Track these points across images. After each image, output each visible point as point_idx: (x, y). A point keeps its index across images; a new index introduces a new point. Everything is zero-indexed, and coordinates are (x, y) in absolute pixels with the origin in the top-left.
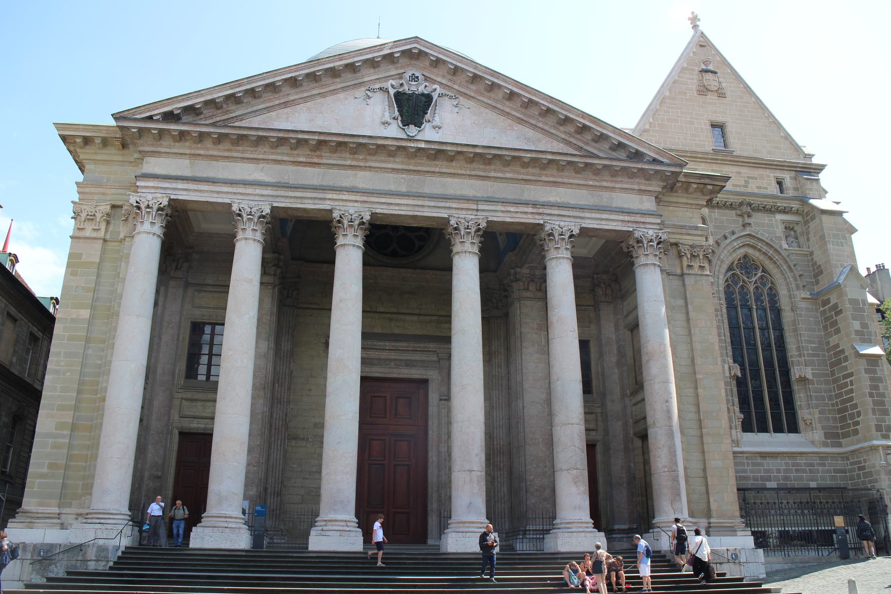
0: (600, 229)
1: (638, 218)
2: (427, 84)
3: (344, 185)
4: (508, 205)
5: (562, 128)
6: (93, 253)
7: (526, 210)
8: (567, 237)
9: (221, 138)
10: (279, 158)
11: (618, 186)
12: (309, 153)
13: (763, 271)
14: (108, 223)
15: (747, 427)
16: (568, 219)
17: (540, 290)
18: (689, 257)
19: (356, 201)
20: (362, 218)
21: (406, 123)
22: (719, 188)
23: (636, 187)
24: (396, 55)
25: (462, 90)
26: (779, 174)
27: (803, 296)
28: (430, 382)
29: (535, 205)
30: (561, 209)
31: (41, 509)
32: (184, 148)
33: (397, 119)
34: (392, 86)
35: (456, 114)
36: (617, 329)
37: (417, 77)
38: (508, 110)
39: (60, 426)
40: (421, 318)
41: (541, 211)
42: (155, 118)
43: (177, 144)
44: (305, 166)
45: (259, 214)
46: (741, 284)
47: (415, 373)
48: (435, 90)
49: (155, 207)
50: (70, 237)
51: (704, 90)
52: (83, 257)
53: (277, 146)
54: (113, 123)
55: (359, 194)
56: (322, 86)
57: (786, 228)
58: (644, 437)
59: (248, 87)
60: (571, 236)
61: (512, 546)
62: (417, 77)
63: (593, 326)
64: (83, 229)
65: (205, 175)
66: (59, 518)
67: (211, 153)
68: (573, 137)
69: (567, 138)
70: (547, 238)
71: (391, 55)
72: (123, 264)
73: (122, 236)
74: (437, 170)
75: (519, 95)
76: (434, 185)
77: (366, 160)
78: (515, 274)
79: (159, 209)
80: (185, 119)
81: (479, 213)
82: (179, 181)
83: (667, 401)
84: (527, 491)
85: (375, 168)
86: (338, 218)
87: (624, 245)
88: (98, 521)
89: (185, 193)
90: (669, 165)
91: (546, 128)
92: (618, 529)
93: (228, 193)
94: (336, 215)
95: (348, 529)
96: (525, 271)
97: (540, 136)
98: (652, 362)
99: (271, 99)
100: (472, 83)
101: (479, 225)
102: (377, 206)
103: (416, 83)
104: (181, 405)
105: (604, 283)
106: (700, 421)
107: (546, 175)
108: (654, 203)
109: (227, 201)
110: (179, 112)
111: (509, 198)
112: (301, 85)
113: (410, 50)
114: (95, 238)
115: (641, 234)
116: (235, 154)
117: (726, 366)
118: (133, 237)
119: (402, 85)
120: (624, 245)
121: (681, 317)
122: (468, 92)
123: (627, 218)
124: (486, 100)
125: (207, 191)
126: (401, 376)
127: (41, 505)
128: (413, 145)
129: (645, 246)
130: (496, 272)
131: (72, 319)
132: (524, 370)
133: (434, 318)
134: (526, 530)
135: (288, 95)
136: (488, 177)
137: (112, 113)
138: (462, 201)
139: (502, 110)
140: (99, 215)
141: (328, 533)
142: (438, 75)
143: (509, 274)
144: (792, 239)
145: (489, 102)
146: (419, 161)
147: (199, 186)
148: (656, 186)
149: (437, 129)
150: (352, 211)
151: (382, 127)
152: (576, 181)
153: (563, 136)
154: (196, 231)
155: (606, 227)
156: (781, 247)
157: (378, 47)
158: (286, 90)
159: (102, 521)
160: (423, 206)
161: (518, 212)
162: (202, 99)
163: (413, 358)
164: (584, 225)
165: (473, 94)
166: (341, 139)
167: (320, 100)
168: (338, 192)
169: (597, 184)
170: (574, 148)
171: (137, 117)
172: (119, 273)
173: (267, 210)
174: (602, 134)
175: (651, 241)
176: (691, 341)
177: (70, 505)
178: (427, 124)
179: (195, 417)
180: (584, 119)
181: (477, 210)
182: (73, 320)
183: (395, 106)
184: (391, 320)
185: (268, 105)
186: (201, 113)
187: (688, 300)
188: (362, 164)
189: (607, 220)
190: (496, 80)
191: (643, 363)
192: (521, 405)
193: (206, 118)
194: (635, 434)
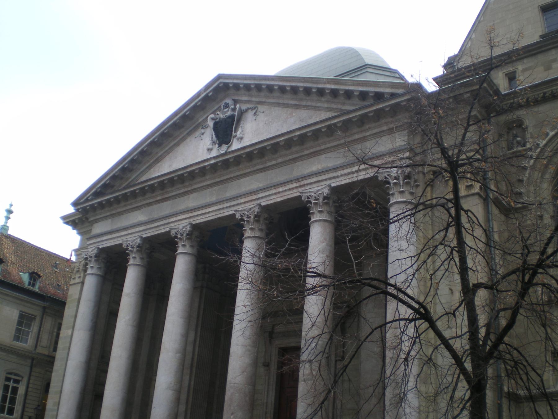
5: (323, 99)
10: (148, 201)
11: (368, 134)
19: (185, 219)
21: (220, 145)
23: (385, 128)
25: (257, 100)
29: (297, 180)
34: (212, 119)
41: (302, 183)
42: (89, 199)
44: (162, 202)
49: (93, 256)
54: (72, 210)
71: (208, 94)
74: (232, 175)
76: (233, 189)
77: (191, 185)
91: (314, 104)
94: (173, 234)
107: (307, 149)
113: (218, 85)
115: (386, 174)
116: (128, 207)
135: (157, 153)
149: (240, 140)
160: (223, 209)
161: (285, 191)
162: (108, 177)
168: (176, 216)
180: (330, 84)
181: (257, 199)
185: (147, 165)
188: (189, 189)
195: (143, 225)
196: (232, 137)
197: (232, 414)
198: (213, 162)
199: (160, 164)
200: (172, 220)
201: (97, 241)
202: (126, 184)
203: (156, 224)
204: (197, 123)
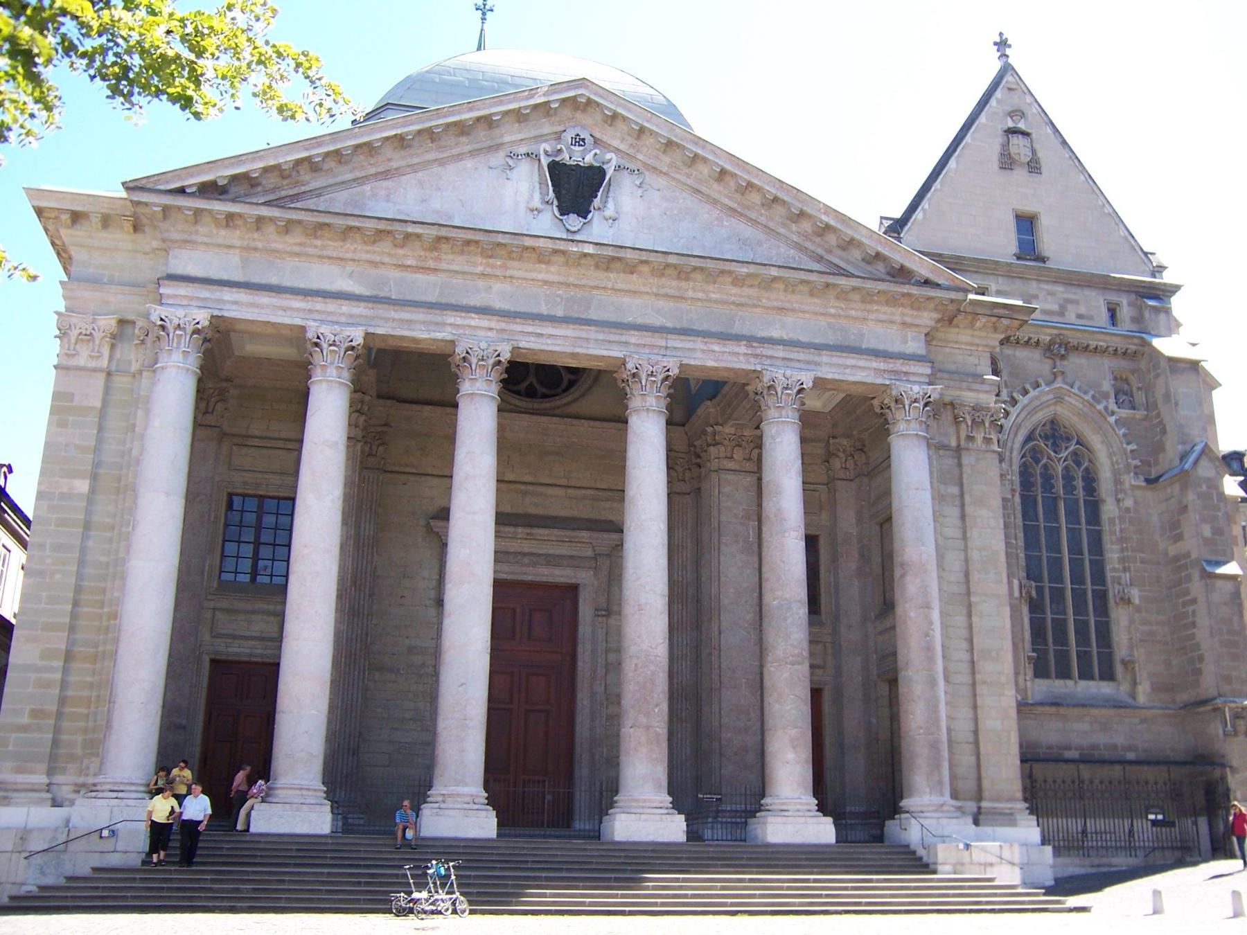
0: (842, 381)
1: (898, 365)
2: (598, 152)
3: (472, 304)
4: (713, 340)
5: (794, 227)
6: (91, 393)
7: (736, 349)
8: (795, 391)
9: (288, 227)
10: (377, 258)
12: (422, 253)
13: (1078, 443)
14: (113, 347)
15: (1041, 671)
16: (797, 365)
17: (750, 459)
18: (970, 424)
19: (491, 329)
20: (499, 355)
21: (564, 211)
22: (1019, 322)
23: (898, 318)
24: (554, 106)
26: (1114, 297)
27: (1133, 483)
28: (581, 589)
30: (787, 348)
31: (21, 778)
34: (546, 152)
35: (639, 199)
36: (859, 521)
37: (583, 140)
38: (716, 196)
39: (48, 654)
40: (570, 491)
41: (758, 351)
44: (415, 272)
45: (347, 344)
46: (1045, 461)
47: (560, 575)
48: (610, 161)
49: (190, 329)
50: (55, 367)
51: (1007, 162)
52: (77, 398)
53: (374, 242)
54: (124, 194)
56: (441, 148)
57: (1115, 379)
58: (893, 682)
59: (332, 148)
60: (800, 391)
61: (697, 832)
62: (583, 140)
63: (824, 515)
65: (264, 281)
66: (48, 791)
67: (274, 245)
68: (811, 240)
69: (800, 241)
70: (765, 392)
71: (549, 102)
72: (140, 413)
73: (134, 367)
75: (734, 175)
78: (714, 434)
80: (234, 190)
81: (668, 353)
82: (226, 288)
83: (927, 635)
84: (721, 754)
87: (876, 402)
88: (115, 795)
89: (234, 307)
90: (948, 289)
91: (771, 225)
92: (851, 813)
93: (299, 310)
94: (460, 350)
95: (476, 807)
96: (728, 429)
97: (762, 236)
98: (908, 578)
100: (664, 152)
101: (668, 370)
102: (521, 338)
103: (581, 148)
104: (213, 619)
105: (844, 451)
106: (973, 662)
107: (768, 299)
108: (923, 345)
109: (298, 322)
110: (225, 182)
112: (410, 146)
113: (575, 97)
114: (95, 370)
115: (902, 389)
116: (310, 251)
117: (1016, 582)
118: (154, 371)
119: (560, 151)
120: (876, 402)
121: (953, 512)
122: (657, 164)
123: (882, 365)
124: (683, 178)
125: (268, 306)
126: (538, 579)
127: (20, 770)
128: (575, 249)
129: (907, 407)
130: (683, 425)
131: (62, 493)
132: (723, 579)
133: (589, 492)
134: (718, 812)
135: (390, 160)
137: (124, 180)
139: (708, 196)
140: (98, 335)
141: (447, 812)
142: (613, 137)
143: (704, 433)
144: (1124, 397)
145: (689, 182)
146: (583, 272)
147: (256, 298)
148: (927, 318)
150: (483, 345)
151: (530, 215)
152: (812, 308)
153: (795, 238)
154: (237, 353)
155: (851, 378)
156: (1106, 408)
157: (526, 93)
158: (388, 151)
159: (120, 795)
162: (261, 165)
163: (557, 552)
164: (820, 375)
165: (665, 169)
166: (470, 236)
167: (436, 169)
168: (463, 314)
169: (842, 313)
170: (811, 257)
171: (162, 187)
172: (134, 425)
173: (359, 340)
174: (852, 240)
175: (916, 401)
176: (966, 549)
177: (64, 771)
178: (597, 213)
179: (235, 637)
182: (63, 496)
184: (525, 493)
185: (358, 174)
186: (258, 184)
187: (965, 488)
188: (499, 272)
189: (853, 367)
190: (700, 152)
191: (896, 579)
192: (716, 628)
193: (266, 192)
194: (879, 676)
195: (362, 304)
197: (657, 705)
199: (385, 184)
200: (451, 320)
201: (202, 296)
202: (291, 192)
203: (405, 315)
204: (500, 141)
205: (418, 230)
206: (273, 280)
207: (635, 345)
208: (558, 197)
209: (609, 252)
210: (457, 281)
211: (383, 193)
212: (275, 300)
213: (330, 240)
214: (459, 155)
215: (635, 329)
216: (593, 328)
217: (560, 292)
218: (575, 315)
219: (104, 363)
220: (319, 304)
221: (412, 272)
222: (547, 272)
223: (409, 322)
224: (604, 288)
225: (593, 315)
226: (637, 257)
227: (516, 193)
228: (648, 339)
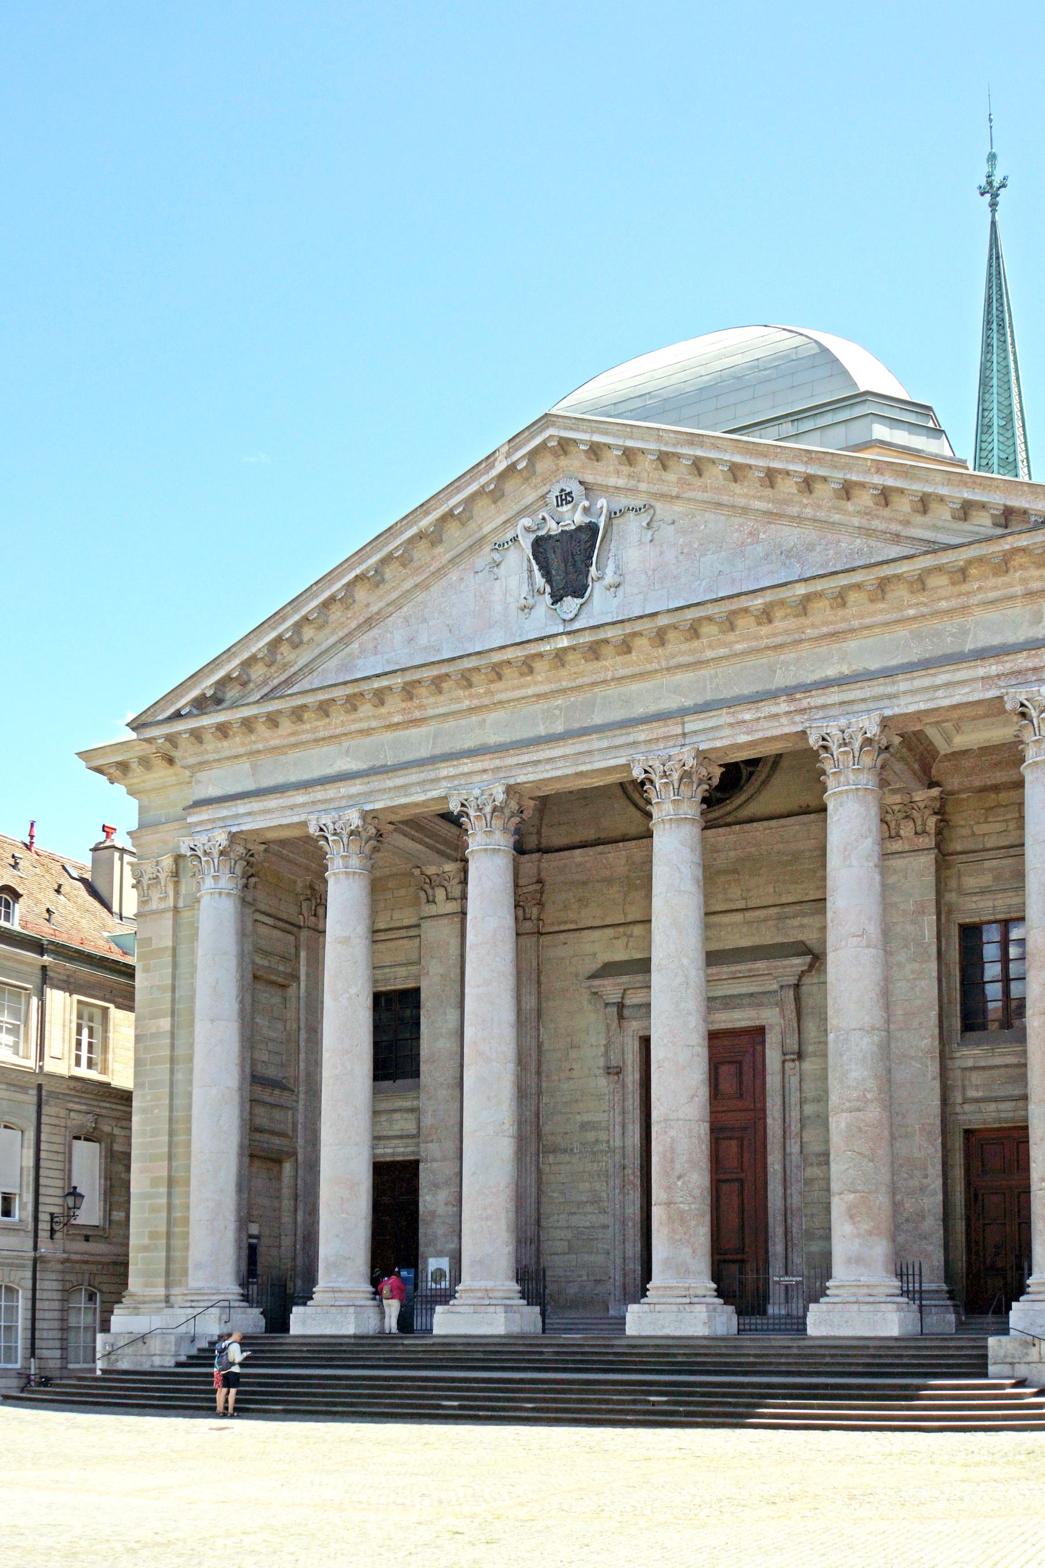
3: (466, 747)
4: (738, 708)
10: (364, 725)
12: (404, 705)
14: (177, 884)
21: (557, 598)
32: (237, 744)
33: (544, 593)
43: (225, 744)
44: (407, 728)
45: (348, 830)
49: (215, 853)
55: (487, 757)
64: (147, 901)
79: (221, 853)
82: (239, 802)
85: (509, 701)
86: (459, 809)
89: (249, 819)
93: (303, 805)
99: (342, 623)
102: (519, 771)
111: (746, 692)
114: (164, 911)
128: (548, 648)
135: (368, 605)
136: (701, 662)
138: (655, 724)
140: (162, 876)
146: (573, 670)
150: (476, 792)
167: (421, 597)
178: (597, 585)
183: (536, 567)
185: (341, 634)
188: (486, 701)
195: (358, 781)
196: (590, 579)
198: (564, 642)
200: (444, 773)
201: (220, 816)
202: (283, 678)
203: (399, 781)
205: (384, 682)
206: (279, 779)
207: (646, 742)
208: (549, 581)
209: (587, 638)
210: (451, 724)
211: (371, 645)
212: (281, 801)
213: (317, 720)
214: (439, 570)
215: (642, 724)
216: (594, 736)
217: (560, 702)
218: (576, 726)
219: (171, 902)
220: (320, 793)
221: (403, 729)
222: (536, 683)
223: (405, 787)
224: (604, 682)
225: (598, 720)
226: (620, 632)
227: (505, 595)
228: (660, 730)
